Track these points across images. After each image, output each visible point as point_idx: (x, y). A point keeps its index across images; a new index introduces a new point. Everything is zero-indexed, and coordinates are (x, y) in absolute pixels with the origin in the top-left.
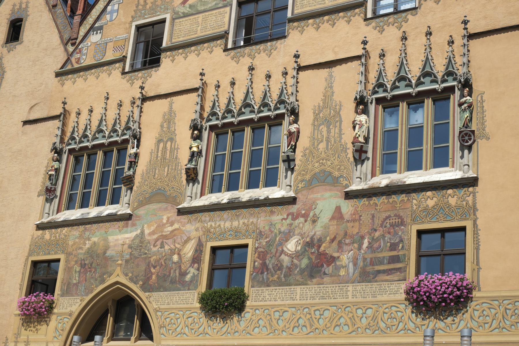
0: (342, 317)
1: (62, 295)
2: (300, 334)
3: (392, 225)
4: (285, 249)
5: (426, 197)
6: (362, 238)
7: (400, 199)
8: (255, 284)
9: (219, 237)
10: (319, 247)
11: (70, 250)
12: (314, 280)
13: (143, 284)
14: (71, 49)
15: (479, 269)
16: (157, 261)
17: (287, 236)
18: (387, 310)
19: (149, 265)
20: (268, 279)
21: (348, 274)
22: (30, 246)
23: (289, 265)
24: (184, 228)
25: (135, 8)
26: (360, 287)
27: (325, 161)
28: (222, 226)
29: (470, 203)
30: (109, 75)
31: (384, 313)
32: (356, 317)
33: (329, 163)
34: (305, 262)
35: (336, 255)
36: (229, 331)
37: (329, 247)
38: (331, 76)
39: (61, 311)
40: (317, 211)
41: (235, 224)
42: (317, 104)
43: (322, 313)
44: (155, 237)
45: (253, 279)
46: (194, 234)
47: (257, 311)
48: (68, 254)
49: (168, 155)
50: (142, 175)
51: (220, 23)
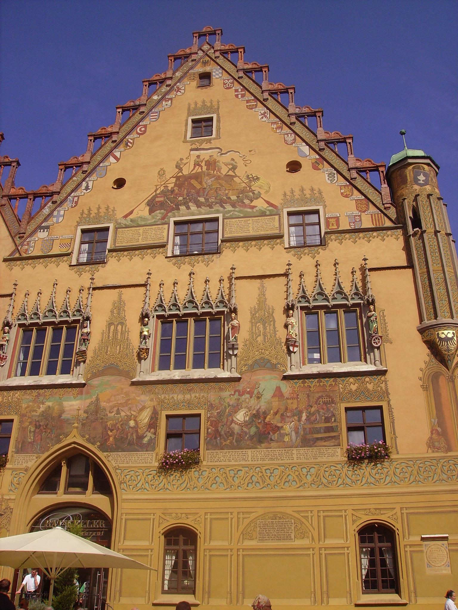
0: (289, 474)
1: (17, 452)
2: (254, 489)
3: (324, 403)
4: (234, 419)
5: (350, 383)
6: (301, 412)
7: (329, 383)
8: (210, 447)
9: (173, 407)
10: (265, 418)
11: (23, 411)
12: (263, 445)
13: (101, 445)
14: (18, 241)
15: (396, 437)
16: (114, 425)
17: (236, 408)
18: (327, 469)
19: (106, 428)
20: (221, 443)
21: (291, 441)
23: (239, 432)
24: (139, 398)
25: (80, 216)
26: (303, 450)
27: (263, 351)
28: (175, 398)
29: (384, 388)
30: (58, 266)
31: (325, 471)
32: (302, 475)
33: (267, 352)
34: (253, 430)
35: (280, 425)
36: (188, 486)
37: (274, 419)
38: (263, 287)
39: (16, 466)
40: (261, 391)
41: (188, 396)
42: (253, 307)
43: (272, 472)
44: (111, 404)
45: (207, 443)
46: (148, 403)
47: (213, 470)
48: (22, 416)
49: (119, 336)
50: (95, 351)
51: (159, 236)
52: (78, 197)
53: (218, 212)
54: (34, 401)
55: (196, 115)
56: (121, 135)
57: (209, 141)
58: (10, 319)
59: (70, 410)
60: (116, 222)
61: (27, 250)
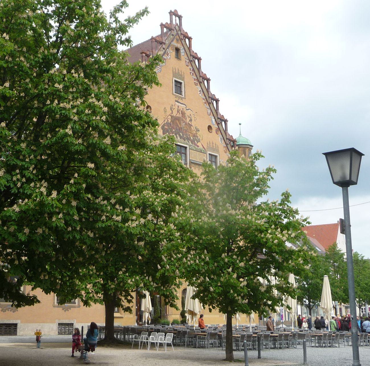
53: (187, 144)
55: (176, 77)
57: (182, 98)
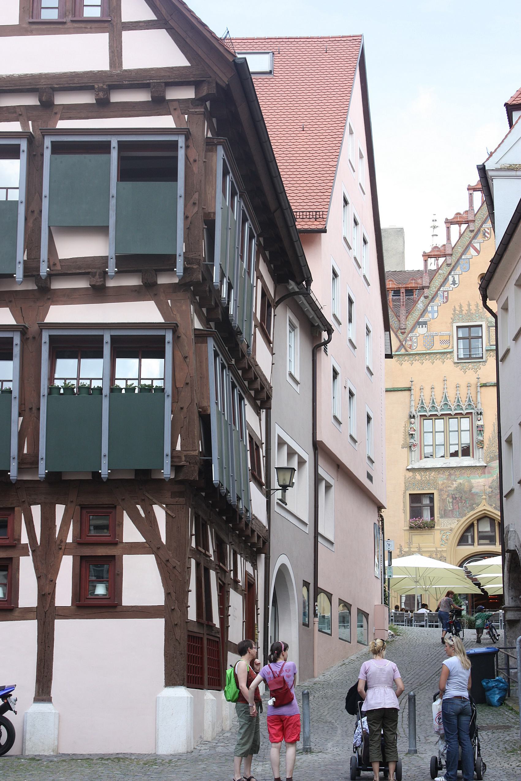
1: (441, 517)
11: (441, 487)
14: (401, 337)
22: (405, 483)
39: (443, 528)
48: (440, 490)
52: (447, 291)
54: (448, 479)
56: (478, 224)
58: (414, 413)
59: (478, 486)
60: (487, 320)
61: (411, 345)
